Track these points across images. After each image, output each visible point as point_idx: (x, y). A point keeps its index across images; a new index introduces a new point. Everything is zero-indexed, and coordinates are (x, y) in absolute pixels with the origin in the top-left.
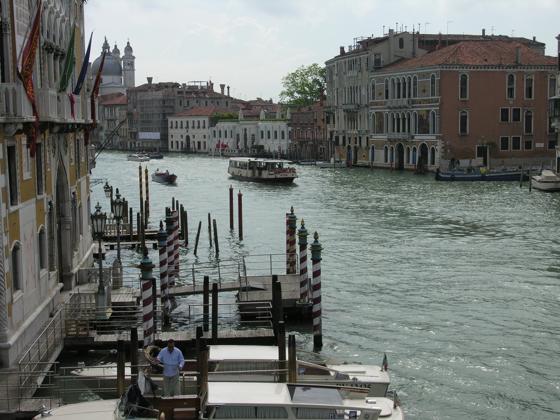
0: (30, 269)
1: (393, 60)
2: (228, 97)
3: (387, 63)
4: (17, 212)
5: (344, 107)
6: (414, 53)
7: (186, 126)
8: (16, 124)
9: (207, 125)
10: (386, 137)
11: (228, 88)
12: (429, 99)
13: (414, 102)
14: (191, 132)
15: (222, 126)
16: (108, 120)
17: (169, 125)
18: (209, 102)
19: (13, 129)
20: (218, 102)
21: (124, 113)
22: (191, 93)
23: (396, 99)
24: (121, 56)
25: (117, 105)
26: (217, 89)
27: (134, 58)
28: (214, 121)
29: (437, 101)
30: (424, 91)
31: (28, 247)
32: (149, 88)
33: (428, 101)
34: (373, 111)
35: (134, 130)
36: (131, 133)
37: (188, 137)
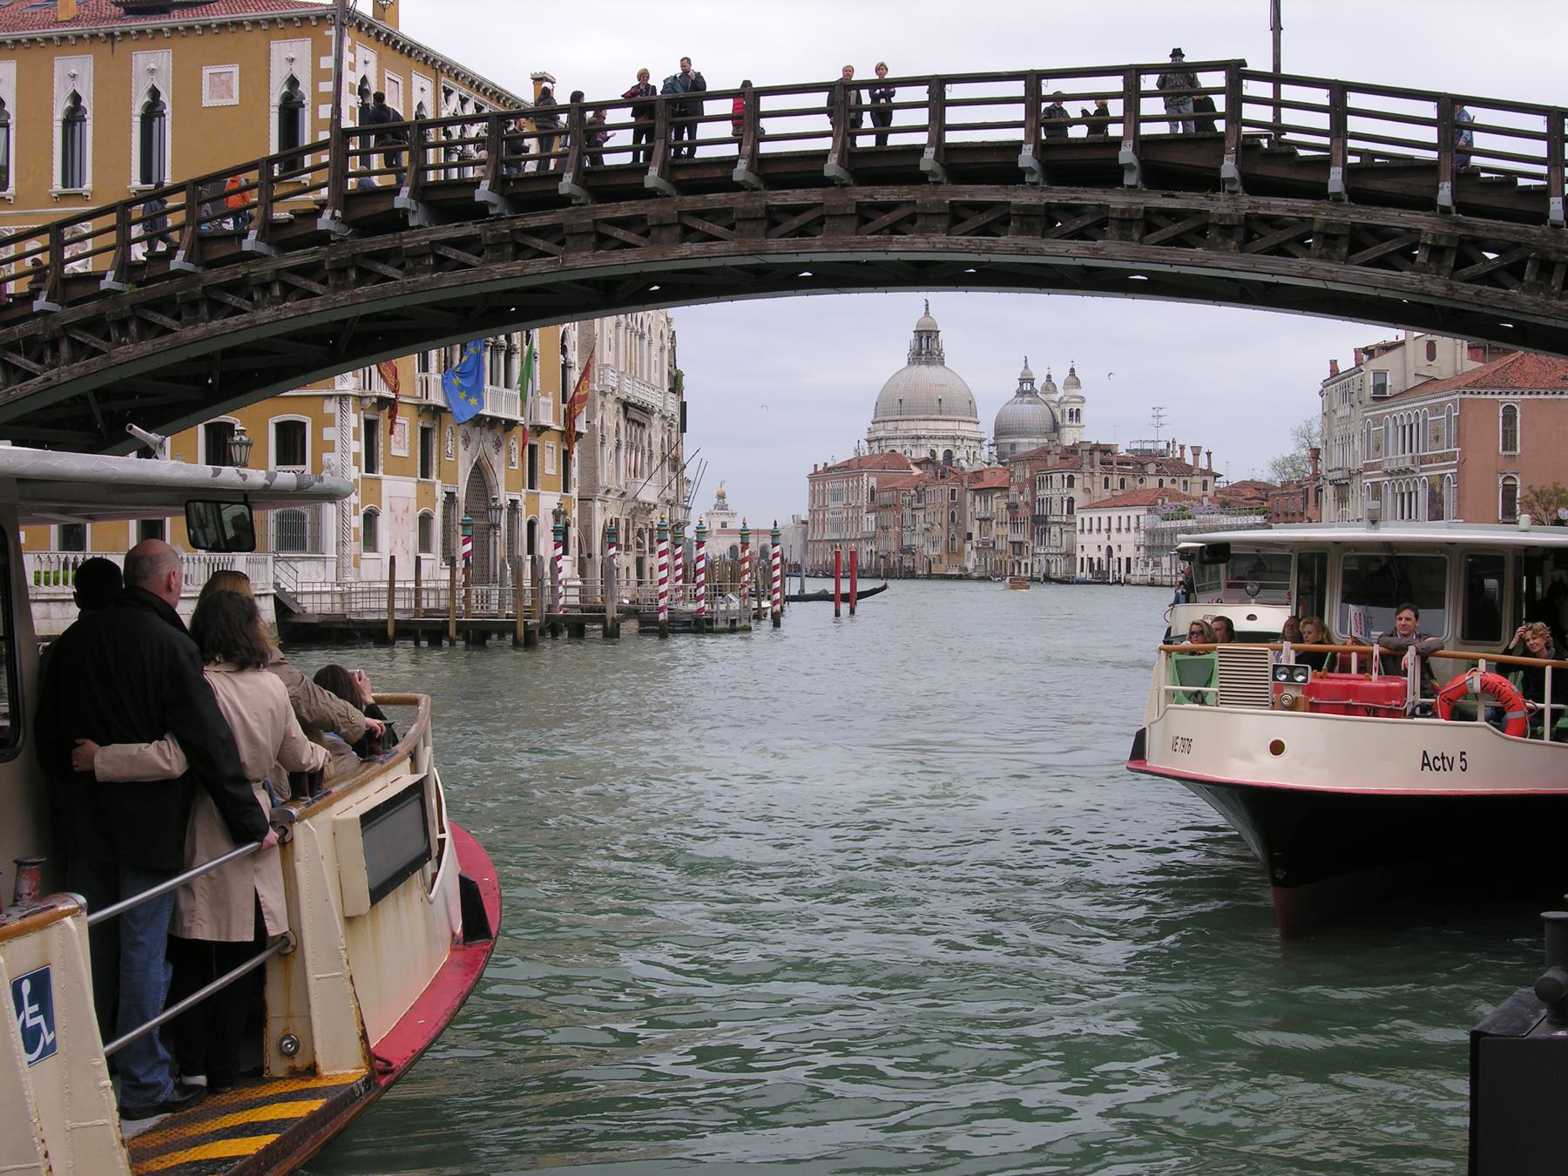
0: (399, 541)
1: (1412, 382)
2: (1208, 472)
3: (1399, 388)
4: (379, 479)
5: (1331, 476)
6: (1456, 373)
7: (1107, 527)
8: (370, 397)
11: (1209, 454)
12: (1443, 454)
13: (1423, 460)
14: (1116, 538)
16: (980, 520)
17: (1079, 527)
19: (367, 403)
20: (1185, 483)
21: (1003, 504)
23: (1400, 455)
24: (1057, 400)
25: (998, 489)
26: (1189, 460)
30: (1437, 438)
32: (1049, 452)
33: (1442, 458)
34: (1368, 480)
35: (1018, 537)
36: (1013, 543)
37: (1110, 549)
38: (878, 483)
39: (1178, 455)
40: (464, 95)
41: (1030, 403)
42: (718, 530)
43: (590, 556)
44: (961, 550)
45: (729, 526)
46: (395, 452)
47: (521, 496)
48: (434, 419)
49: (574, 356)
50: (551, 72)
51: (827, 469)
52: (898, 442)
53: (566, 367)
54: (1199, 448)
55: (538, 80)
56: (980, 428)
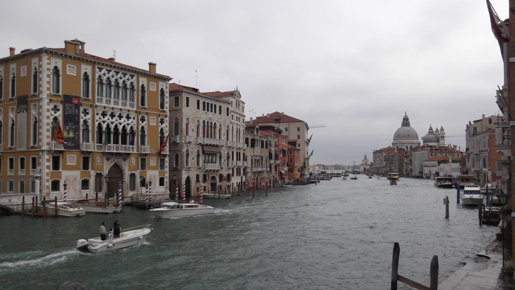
1: (484, 130)
4: (61, 172)
9: (437, 165)
10: (473, 170)
11: (460, 147)
13: (482, 151)
15: (442, 165)
18: (448, 154)
19: (52, 152)
20: (453, 155)
22: (438, 150)
27: (445, 134)
28: (439, 163)
29: (487, 151)
31: (70, 182)
32: (418, 147)
37: (430, 171)
38: (387, 154)
39: (453, 147)
40: (109, 69)
41: (431, 135)
42: (364, 165)
43: (181, 185)
44: (402, 171)
45: (367, 163)
46: (68, 164)
47: (137, 173)
48: (90, 154)
49: (166, 134)
50: (153, 62)
51: (377, 151)
52: (399, 144)
53: (162, 137)
54: (456, 146)
55: (150, 64)
56: (419, 141)
